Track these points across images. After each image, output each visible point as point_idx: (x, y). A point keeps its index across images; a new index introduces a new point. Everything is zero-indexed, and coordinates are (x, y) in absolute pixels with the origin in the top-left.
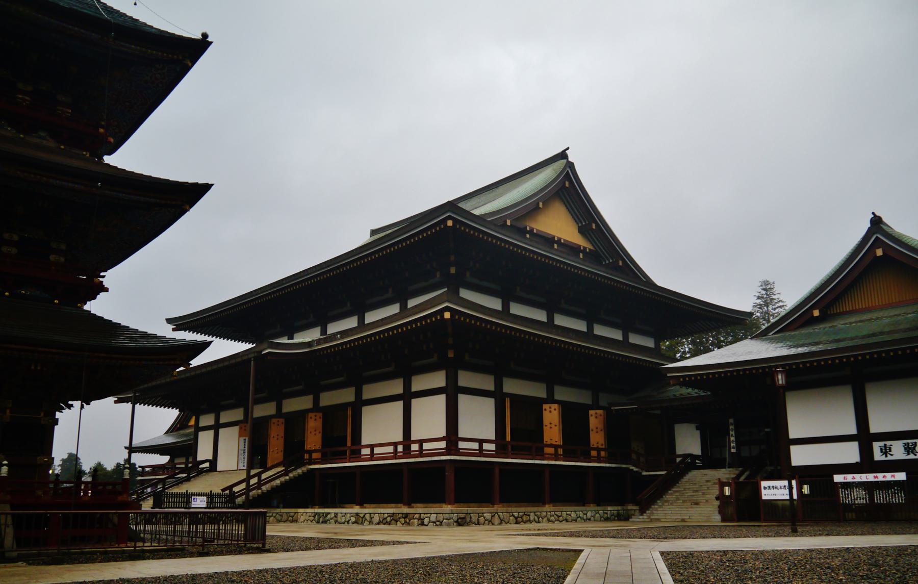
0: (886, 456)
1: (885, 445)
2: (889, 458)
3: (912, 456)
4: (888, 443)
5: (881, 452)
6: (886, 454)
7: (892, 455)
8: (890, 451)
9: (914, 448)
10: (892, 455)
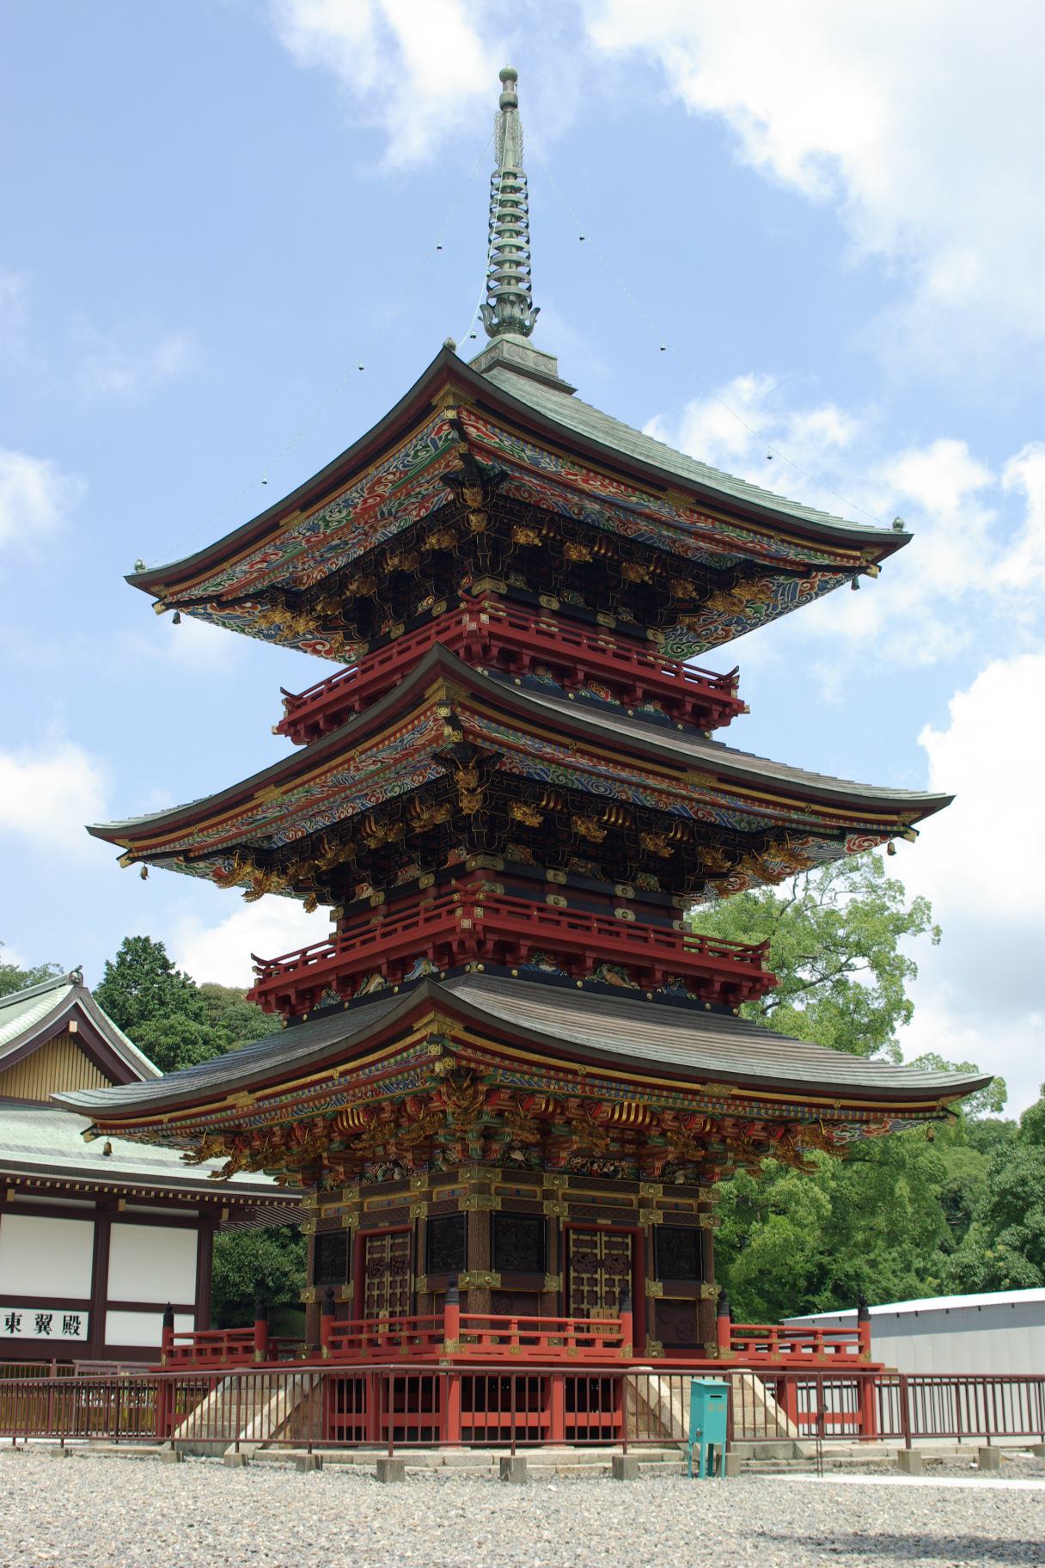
0: (12, 1332)
1: (13, 1314)
2: (16, 1335)
3: (43, 1335)
4: (18, 1312)
5: (7, 1324)
6: (12, 1327)
7: (19, 1331)
8: (18, 1324)
9: (48, 1323)
10: (19, 1331)
